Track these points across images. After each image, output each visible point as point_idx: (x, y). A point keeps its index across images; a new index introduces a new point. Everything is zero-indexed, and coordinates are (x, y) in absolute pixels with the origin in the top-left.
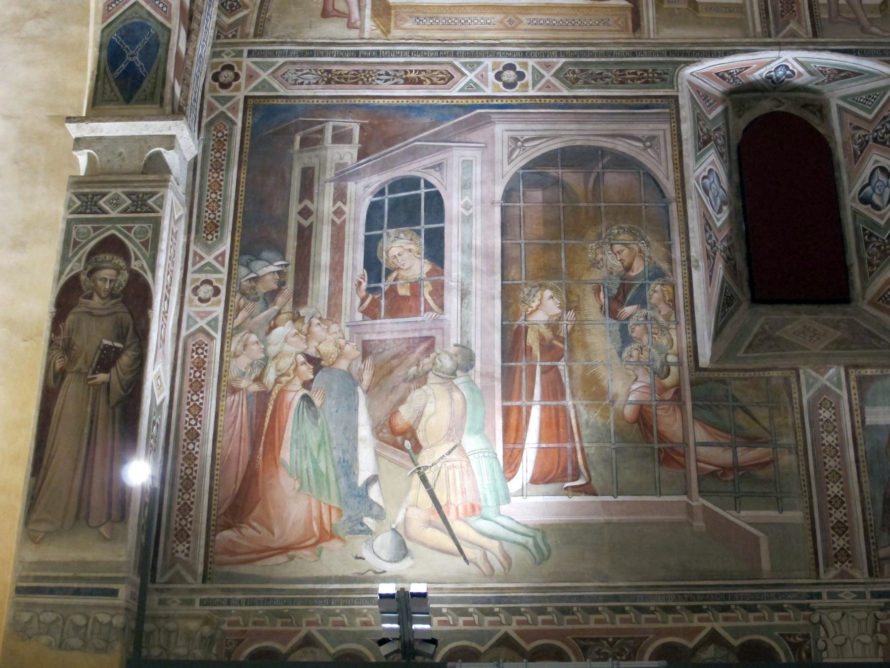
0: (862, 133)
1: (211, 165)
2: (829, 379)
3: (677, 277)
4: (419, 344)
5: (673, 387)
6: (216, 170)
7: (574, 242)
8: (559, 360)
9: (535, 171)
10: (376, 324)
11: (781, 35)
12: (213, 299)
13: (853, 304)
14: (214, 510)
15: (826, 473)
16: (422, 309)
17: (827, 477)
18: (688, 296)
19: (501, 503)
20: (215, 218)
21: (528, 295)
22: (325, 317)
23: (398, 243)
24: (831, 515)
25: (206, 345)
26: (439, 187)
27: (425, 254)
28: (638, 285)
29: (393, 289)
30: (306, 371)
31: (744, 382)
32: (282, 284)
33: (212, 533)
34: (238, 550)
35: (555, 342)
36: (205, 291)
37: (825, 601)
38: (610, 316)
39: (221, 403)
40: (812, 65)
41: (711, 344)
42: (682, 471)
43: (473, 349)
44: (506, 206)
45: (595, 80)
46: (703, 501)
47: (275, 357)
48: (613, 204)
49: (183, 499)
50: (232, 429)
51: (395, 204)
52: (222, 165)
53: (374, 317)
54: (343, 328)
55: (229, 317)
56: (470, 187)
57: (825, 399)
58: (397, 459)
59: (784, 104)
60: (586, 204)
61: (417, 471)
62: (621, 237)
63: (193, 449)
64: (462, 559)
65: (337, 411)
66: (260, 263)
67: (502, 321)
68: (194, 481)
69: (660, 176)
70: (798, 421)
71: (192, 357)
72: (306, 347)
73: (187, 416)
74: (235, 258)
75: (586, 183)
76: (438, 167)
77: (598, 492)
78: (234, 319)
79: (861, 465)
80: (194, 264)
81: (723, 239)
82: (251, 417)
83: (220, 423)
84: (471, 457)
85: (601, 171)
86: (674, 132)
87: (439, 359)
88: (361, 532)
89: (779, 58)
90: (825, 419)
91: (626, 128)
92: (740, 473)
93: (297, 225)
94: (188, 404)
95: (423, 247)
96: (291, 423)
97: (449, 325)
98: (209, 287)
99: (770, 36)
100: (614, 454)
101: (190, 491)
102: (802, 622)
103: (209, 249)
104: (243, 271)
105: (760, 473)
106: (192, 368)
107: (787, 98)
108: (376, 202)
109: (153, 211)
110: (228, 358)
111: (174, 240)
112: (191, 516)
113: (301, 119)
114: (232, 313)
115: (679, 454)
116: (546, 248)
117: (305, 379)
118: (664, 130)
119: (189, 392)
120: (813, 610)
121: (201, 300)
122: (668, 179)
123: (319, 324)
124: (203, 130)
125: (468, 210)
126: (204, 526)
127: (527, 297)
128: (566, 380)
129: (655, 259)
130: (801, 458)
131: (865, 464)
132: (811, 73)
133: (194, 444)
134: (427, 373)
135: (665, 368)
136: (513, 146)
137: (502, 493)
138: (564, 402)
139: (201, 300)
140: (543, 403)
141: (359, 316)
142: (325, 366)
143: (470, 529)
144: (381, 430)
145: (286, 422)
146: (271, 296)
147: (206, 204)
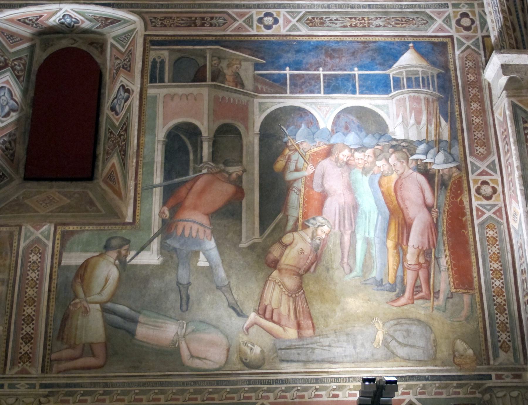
0: (119, 61)
2: (42, 233)
13: (95, 181)
15: (25, 299)
17: (25, 302)
24: (23, 329)
40: (87, 14)
57: (36, 247)
59: (77, 42)
70: (13, 263)
79: (52, 293)
81: (6, 135)
89: (61, 9)
90: (32, 261)
107: (80, 38)
130: (9, 288)
131: (55, 293)
132: (90, 21)
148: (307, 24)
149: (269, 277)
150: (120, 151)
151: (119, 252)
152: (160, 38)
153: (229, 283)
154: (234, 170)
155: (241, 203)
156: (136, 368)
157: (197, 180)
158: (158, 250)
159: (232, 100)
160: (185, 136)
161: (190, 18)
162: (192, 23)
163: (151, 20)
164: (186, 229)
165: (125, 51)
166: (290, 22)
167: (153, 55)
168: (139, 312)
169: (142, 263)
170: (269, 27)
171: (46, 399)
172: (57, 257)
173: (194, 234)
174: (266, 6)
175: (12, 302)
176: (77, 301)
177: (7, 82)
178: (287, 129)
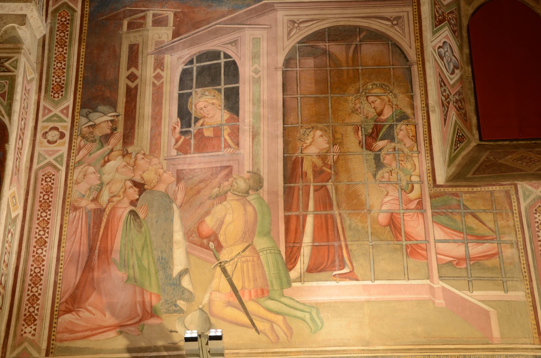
1: (57, 42)
3: (418, 119)
4: (220, 172)
6: (61, 46)
7: (338, 95)
8: (327, 181)
9: (308, 44)
10: (188, 157)
12: (59, 141)
14: (58, 299)
16: (223, 146)
18: (427, 133)
19: (284, 287)
20: (60, 82)
21: (304, 135)
22: (148, 153)
23: (204, 98)
25: (53, 175)
26: (235, 58)
27: (225, 106)
29: (200, 132)
30: (133, 193)
32: (114, 130)
33: (55, 317)
34: (76, 329)
35: (324, 168)
36: (53, 135)
38: (366, 149)
39: (65, 218)
41: (446, 169)
42: (425, 261)
43: (262, 174)
44: (286, 71)
46: (442, 284)
47: (108, 184)
48: (368, 67)
49: (32, 292)
50: (73, 237)
51: (201, 71)
52: (66, 42)
53: (186, 153)
54: (162, 161)
55: (72, 155)
56: (259, 57)
58: (204, 256)
60: (347, 68)
61: (219, 265)
62: (375, 91)
63: (42, 253)
64: (254, 330)
65: (157, 222)
66: (97, 114)
67: (284, 153)
68: (42, 277)
69: (405, 46)
70: (518, 224)
71: (42, 184)
72: (133, 175)
73: (37, 228)
74: (77, 110)
75: (347, 52)
76: (234, 43)
77: (359, 277)
78: (76, 156)
80: (43, 116)
81: (456, 94)
82: (89, 228)
83: (64, 233)
84: (261, 254)
85: (358, 43)
86: (415, 13)
87: (235, 182)
88: (175, 311)
91: (378, 11)
92: (472, 263)
93: (125, 87)
94: (38, 219)
95: (223, 101)
96: (121, 232)
97: (243, 158)
98: (56, 133)
100: (371, 250)
101: (38, 285)
103: (56, 104)
104: (84, 120)
106: (41, 193)
108: (186, 69)
109: (9, 71)
110: (71, 185)
111: (27, 95)
112: (38, 305)
113: (128, 8)
114: (75, 151)
115: (423, 249)
116: (317, 100)
117: (132, 199)
119: (39, 210)
121: (49, 142)
122: (410, 48)
123: (143, 158)
124: (49, 15)
125: (257, 74)
126: (49, 311)
127: (302, 136)
129: (400, 107)
130: (521, 251)
133: (42, 249)
134: (227, 192)
135: (410, 185)
136: (291, 27)
137: (284, 280)
138: (332, 212)
139: (49, 142)
140: (316, 213)
141: (174, 152)
142: (148, 189)
143: (260, 307)
144: (191, 235)
145: (117, 231)
146: (106, 138)
147: (53, 71)
175: (528, 265)
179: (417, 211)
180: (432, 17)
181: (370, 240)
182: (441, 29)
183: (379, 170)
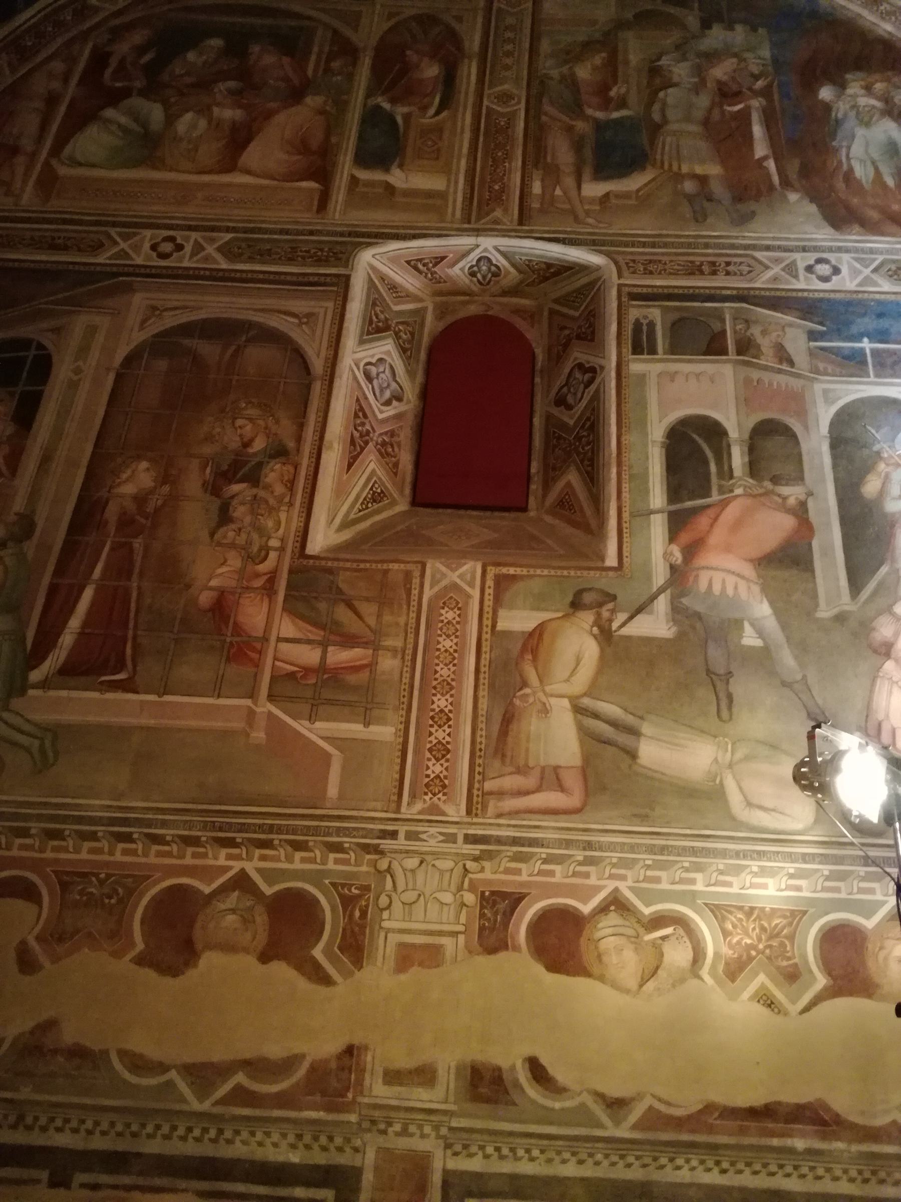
0: (567, 332)
2: (461, 577)
5: (265, 574)
8: (136, 537)
11: (483, 221)
15: (435, 683)
17: (435, 688)
24: (431, 734)
28: (253, 463)
31: (355, 574)
35: (138, 517)
37: (401, 842)
42: (254, 670)
45: (261, 255)
57: (451, 597)
62: (249, 412)
69: (310, 352)
70: (412, 622)
76: (57, 330)
79: (482, 676)
81: (386, 433)
89: (478, 246)
90: (446, 621)
92: (326, 676)
99: (469, 222)
102: (364, 868)
105: (352, 679)
115: (254, 649)
118: (327, 308)
120: (382, 853)
122: (318, 356)
128: (138, 559)
130: (406, 663)
135: (263, 553)
148: (891, 276)
149: (878, 671)
150: (582, 461)
151: (599, 615)
152: (645, 290)
153: (804, 677)
154: (792, 493)
155: (810, 545)
156: (644, 818)
157: (727, 505)
158: (667, 614)
159: (775, 384)
160: (699, 435)
161: (692, 262)
162: (695, 270)
163: (627, 264)
164: (714, 581)
165: (581, 315)
166: (860, 272)
167: (634, 313)
168: (642, 718)
169: (640, 634)
170: (826, 279)
171: (476, 864)
172: (488, 615)
173: (730, 592)
174: (816, 249)
175: (412, 687)
176: (527, 691)
177: (388, 353)
178: (877, 432)
179: (263, 591)
180: (364, 319)
181: (175, 630)
182: (379, 339)
183: (222, 526)
